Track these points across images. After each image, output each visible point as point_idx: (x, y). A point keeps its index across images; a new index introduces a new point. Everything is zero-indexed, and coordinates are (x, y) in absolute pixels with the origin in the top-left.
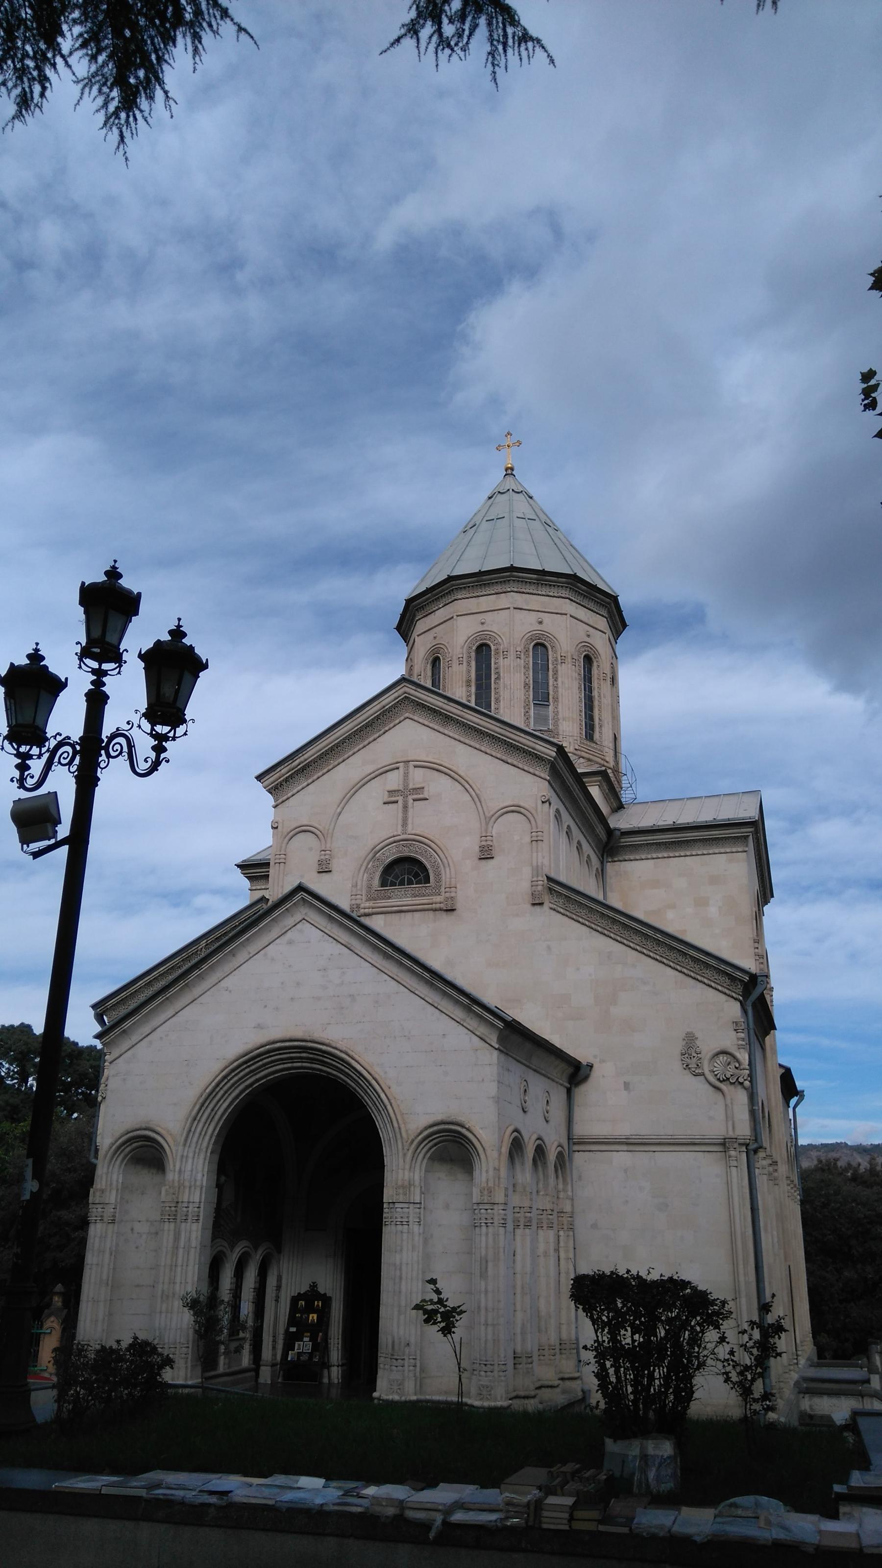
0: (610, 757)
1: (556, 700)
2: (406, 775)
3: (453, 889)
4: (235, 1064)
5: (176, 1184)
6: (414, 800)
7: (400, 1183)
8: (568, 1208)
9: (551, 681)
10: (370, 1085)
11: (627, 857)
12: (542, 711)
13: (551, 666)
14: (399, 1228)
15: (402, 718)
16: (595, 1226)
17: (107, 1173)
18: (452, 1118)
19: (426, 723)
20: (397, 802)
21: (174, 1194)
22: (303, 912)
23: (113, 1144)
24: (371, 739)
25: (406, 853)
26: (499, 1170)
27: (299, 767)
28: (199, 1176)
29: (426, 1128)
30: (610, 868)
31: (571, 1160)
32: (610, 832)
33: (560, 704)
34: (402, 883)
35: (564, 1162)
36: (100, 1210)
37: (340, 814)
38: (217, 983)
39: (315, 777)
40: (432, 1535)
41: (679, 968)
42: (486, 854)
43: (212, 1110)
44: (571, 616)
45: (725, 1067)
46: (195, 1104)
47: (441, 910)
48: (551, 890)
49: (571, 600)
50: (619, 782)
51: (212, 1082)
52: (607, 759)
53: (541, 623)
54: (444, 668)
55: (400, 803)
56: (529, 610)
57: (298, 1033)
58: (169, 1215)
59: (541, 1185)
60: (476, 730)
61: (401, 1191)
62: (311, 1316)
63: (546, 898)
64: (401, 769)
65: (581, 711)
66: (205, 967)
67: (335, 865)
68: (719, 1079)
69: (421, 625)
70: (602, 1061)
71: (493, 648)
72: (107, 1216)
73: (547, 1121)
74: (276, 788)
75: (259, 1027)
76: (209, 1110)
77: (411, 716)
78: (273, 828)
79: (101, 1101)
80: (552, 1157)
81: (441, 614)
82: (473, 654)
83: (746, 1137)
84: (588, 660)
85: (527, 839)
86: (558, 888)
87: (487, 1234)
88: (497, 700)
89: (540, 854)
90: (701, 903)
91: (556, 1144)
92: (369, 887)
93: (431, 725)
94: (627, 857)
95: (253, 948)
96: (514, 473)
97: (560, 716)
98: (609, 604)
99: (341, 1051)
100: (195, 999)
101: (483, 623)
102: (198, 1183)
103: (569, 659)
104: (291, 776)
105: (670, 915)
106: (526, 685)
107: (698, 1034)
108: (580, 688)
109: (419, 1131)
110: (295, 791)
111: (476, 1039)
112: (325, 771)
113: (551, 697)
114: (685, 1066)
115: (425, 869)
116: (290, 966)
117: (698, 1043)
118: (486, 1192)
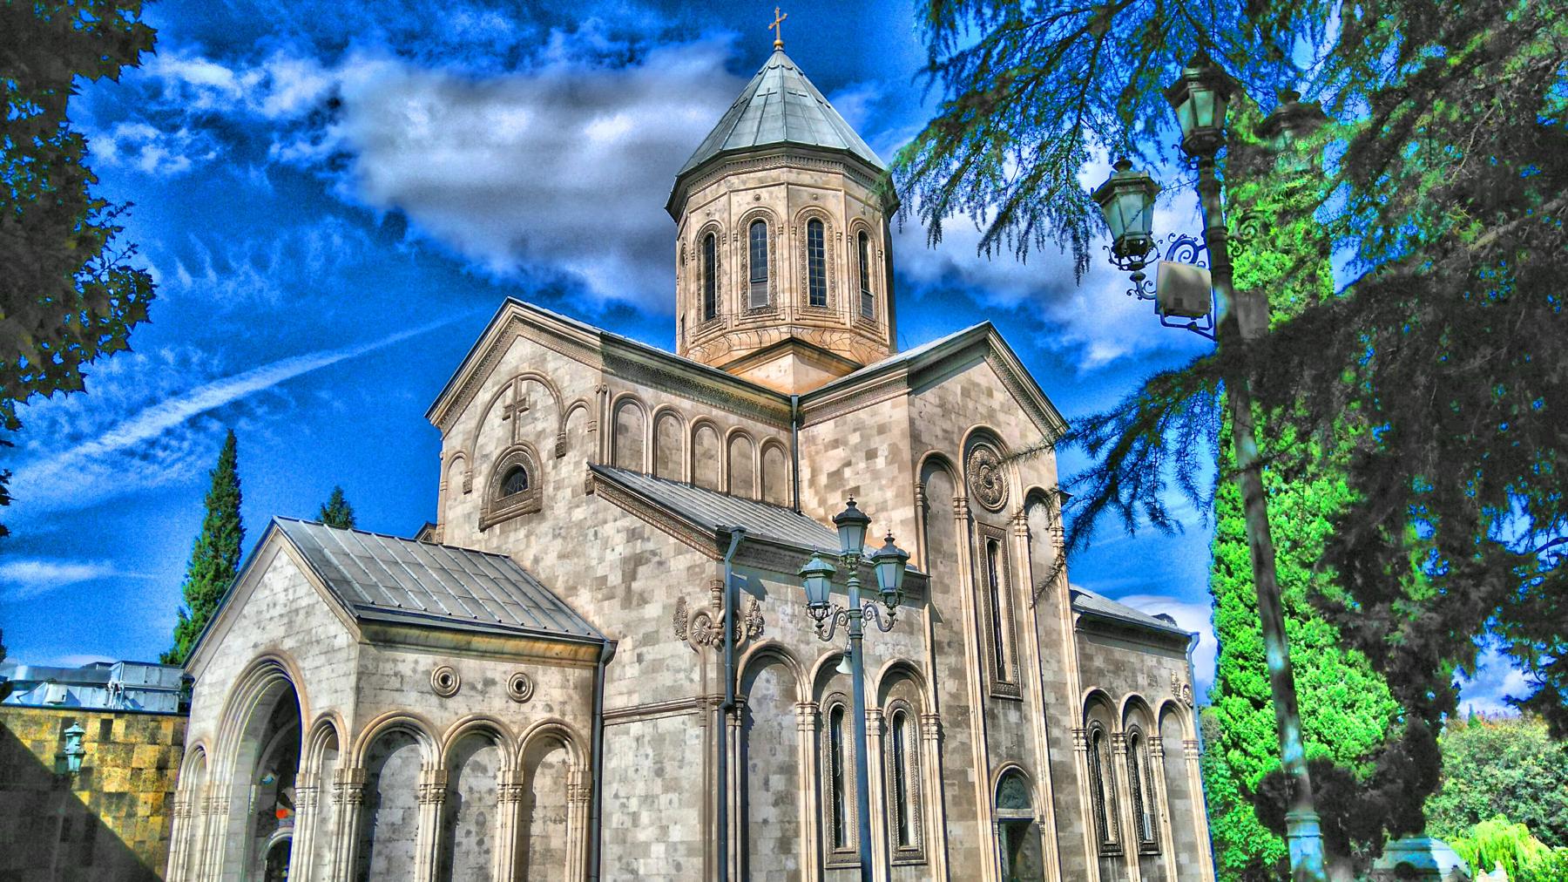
1: (774, 274)
13: (768, 241)
16: (616, 796)
26: (350, 753)
32: (788, 400)
42: (560, 452)
53: (758, 199)
67: (474, 487)
70: (625, 636)
75: (255, 646)
88: (719, 288)
90: (871, 455)
103: (786, 230)
104: (449, 410)
105: (847, 472)
106: (744, 266)
108: (802, 256)
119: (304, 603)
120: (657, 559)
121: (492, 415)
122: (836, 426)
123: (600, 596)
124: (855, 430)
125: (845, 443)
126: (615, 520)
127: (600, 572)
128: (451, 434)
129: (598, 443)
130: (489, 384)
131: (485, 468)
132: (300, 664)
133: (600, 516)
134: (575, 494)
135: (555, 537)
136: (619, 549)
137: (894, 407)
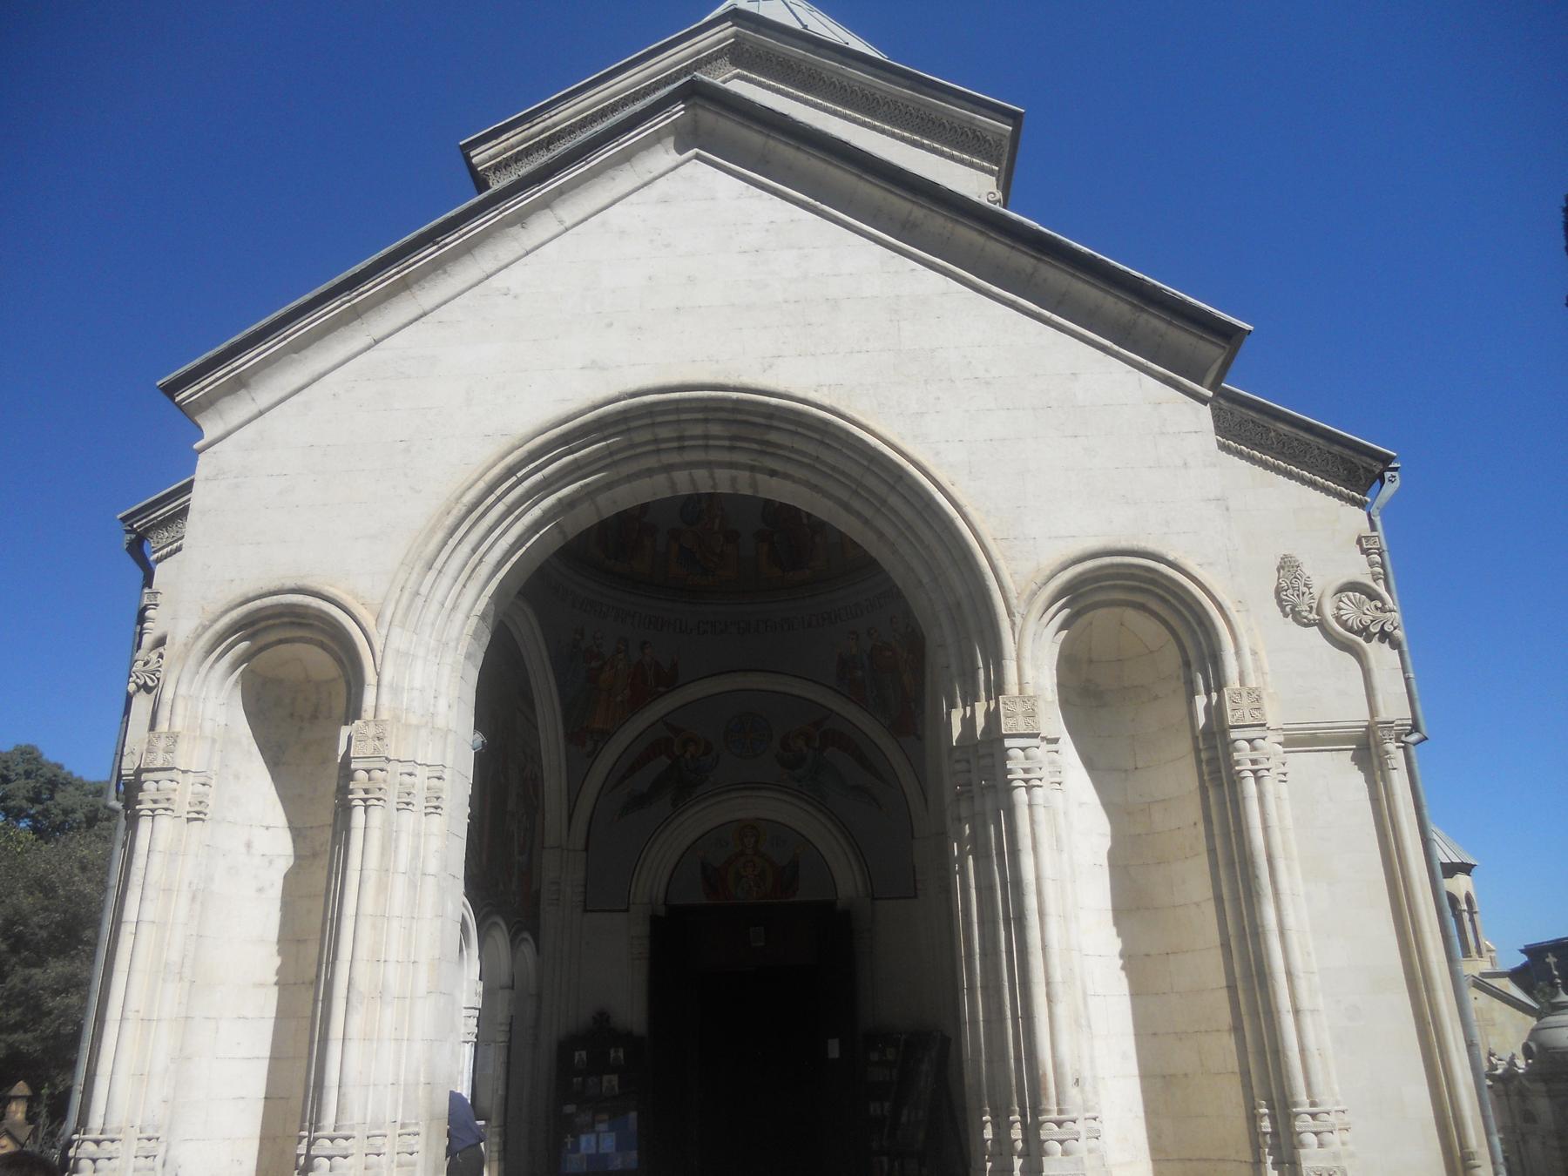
18: (1124, 544)
21: (379, 739)
23: (205, 628)
27: (542, 137)
29: (1065, 567)
36: (165, 784)
38: (480, 282)
43: (474, 551)
45: (1358, 608)
46: (433, 531)
51: (476, 481)
58: (366, 791)
61: (1019, 709)
62: (606, 1078)
66: (453, 240)
68: (1350, 630)
72: (183, 804)
79: (134, 693)
83: (1405, 722)
95: (570, 210)
100: (425, 314)
109: (1048, 572)
114: (1288, 609)
116: (667, 246)
117: (1307, 570)
118: (1245, 701)
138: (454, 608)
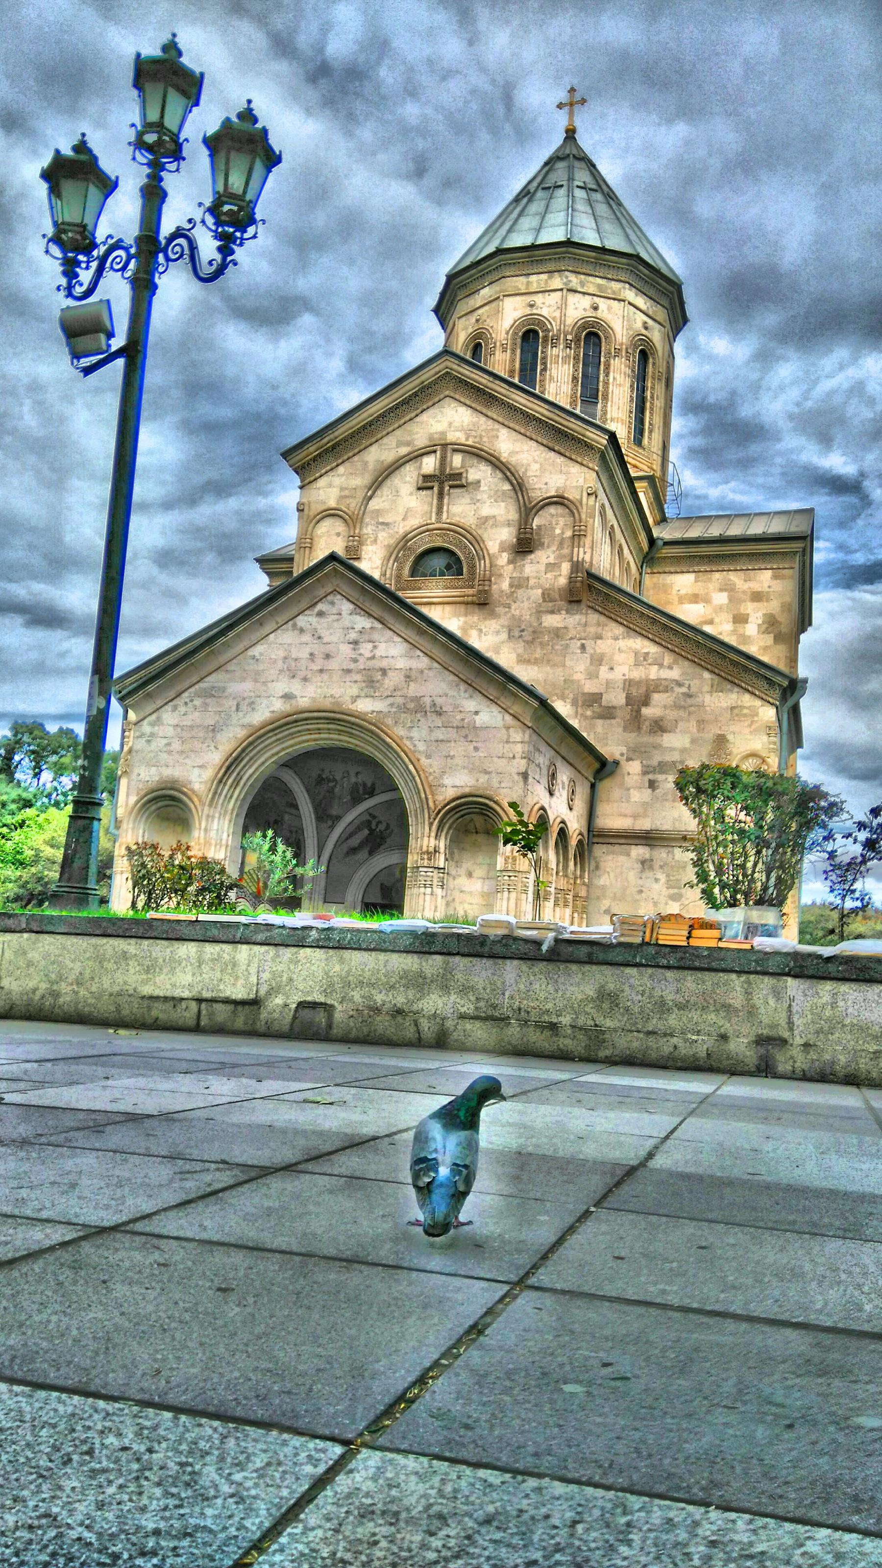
0: (657, 467)
1: (606, 397)
2: (443, 459)
3: (487, 583)
4: (262, 731)
5: (202, 841)
6: (451, 487)
7: (425, 849)
8: (583, 893)
9: (601, 378)
10: (399, 756)
11: (667, 569)
12: (590, 409)
13: (602, 359)
14: (422, 890)
15: (442, 396)
17: (133, 829)
18: (480, 792)
19: (468, 402)
20: (432, 488)
22: (336, 582)
24: (407, 418)
25: (439, 543)
28: (225, 836)
30: (648, 580)
31: (590, 851)
32: (652, 541)
33: (609, 403)
34: (433, 575)
35: (583, 851)
37: (370, 498)
39: (345, 457)
40: (545, 948)
41: (716, 671)
44: (630, 303)
47: (473, 603)
48: (590, 587)
49: (631, 285)
50: (665, 496)
52: (654, 467)
53: (596, 308)
54: (486, 356)
55: (436, 489)
56: (584, 293)
57: (327, 704)
59: (561, 867)
60: (523, 413)
63: (585, 596)
64: (438, 453)
65: (631, 412)
66: (231, 634)
69: (462, 307)
70: (629, 759)
71: (541, 334)
73: (571, 809)
74: (303, 467)
75: (287, 697)
76: (235, 774)
77: (452, 394)
78: (298, 510)
80: (573, 842)
81: (486, 293)
82: (519, 341)
84: (644, 355)
85: (569, 533)
86: (597, 585)
87: (508, 899)
89: (581, 549)
91: (577, 832)
92: (399, 577)
93: (473, 405)
94: (667, 569)
96: (576, 136)
97: (609, 416)
98: (672, 293)
99: (370, 723)
101: (532, 306)
102: (224, 842)
104: (319, 455)
106: (575, 378)
107: (730, 737)
110: (323, 471)
111: (508, 718)
112: (356, 451)
113: (600, 394)
115: (458, 561)
116: (319, 638)
119: (401, 663)
120: (684, 690)
121: (396, 480)
122: (696, 581)
123: (589, 713)
124: (721, 590)
125: (707, 600)
126: (616, 639)
127: (590, 687)
128: (314, 485)
129: (588, 551)
130: (390, 441)
131: (386, 538)
132: (400, 731)
133: (592, 630)
134: (547, 596)
135: (510, 637)
136: (624, 669)
137: (775, 577)
138: (231, 797)
